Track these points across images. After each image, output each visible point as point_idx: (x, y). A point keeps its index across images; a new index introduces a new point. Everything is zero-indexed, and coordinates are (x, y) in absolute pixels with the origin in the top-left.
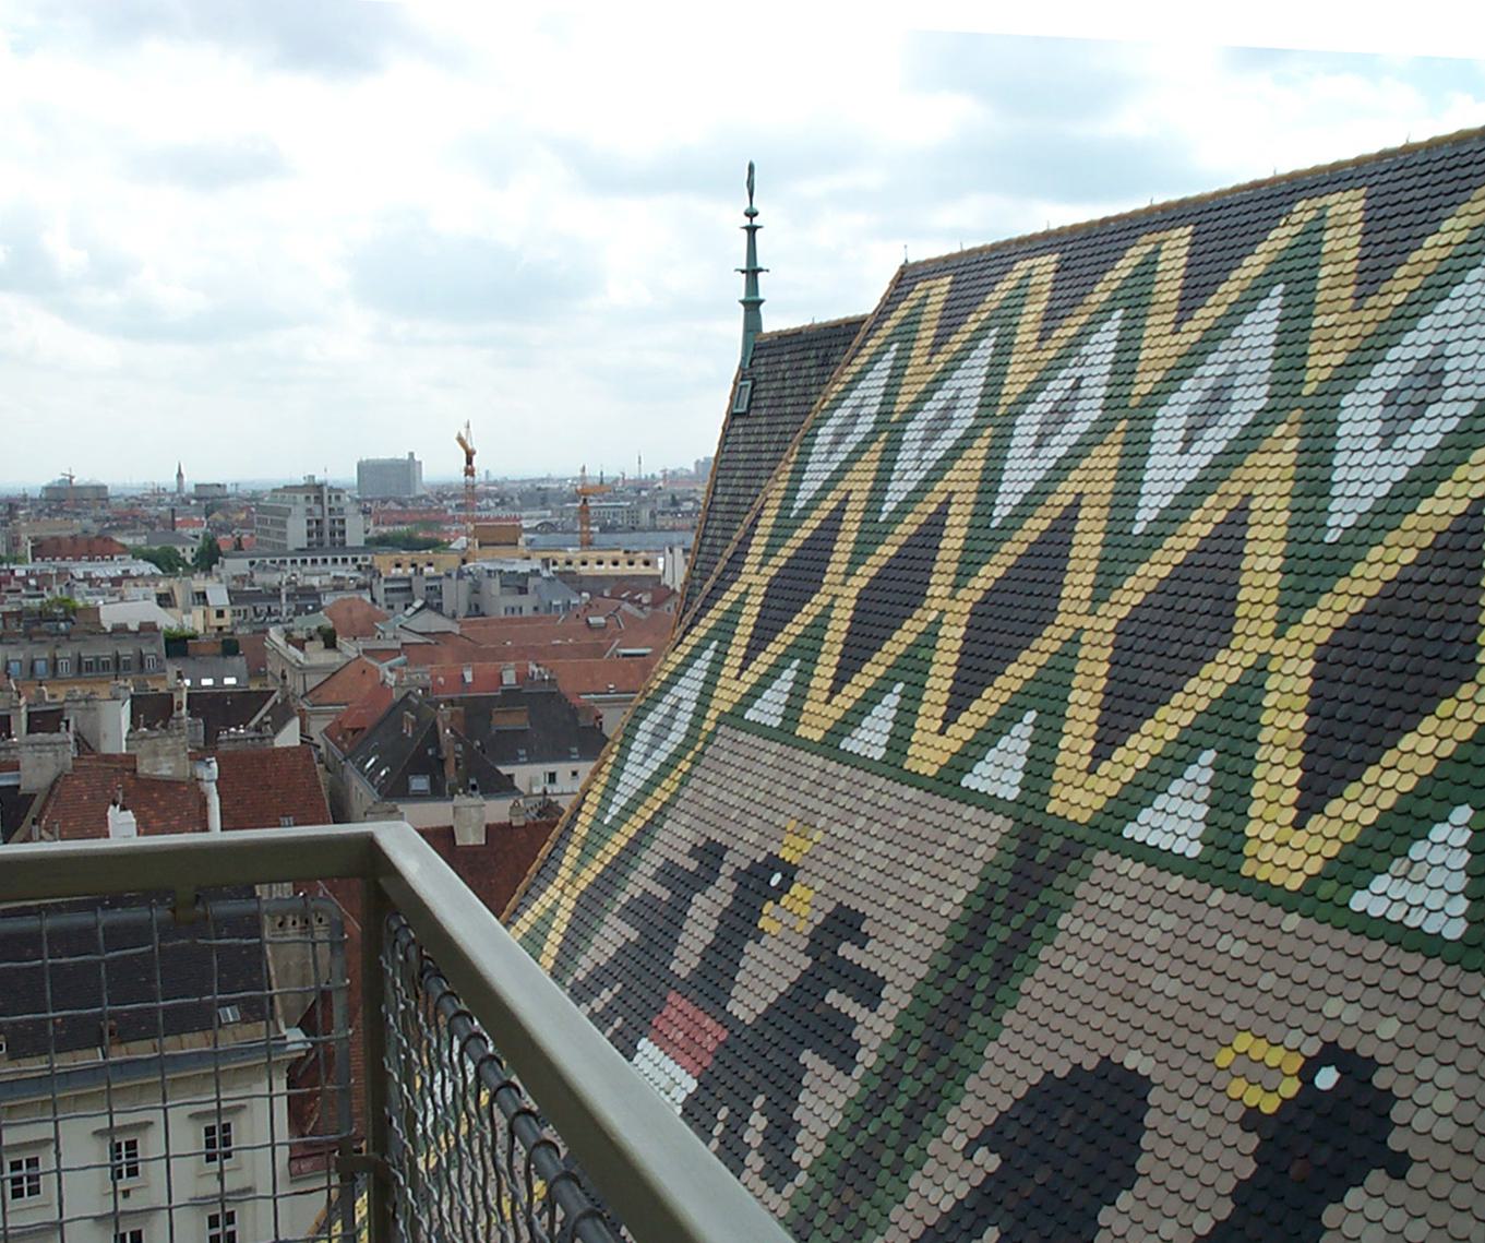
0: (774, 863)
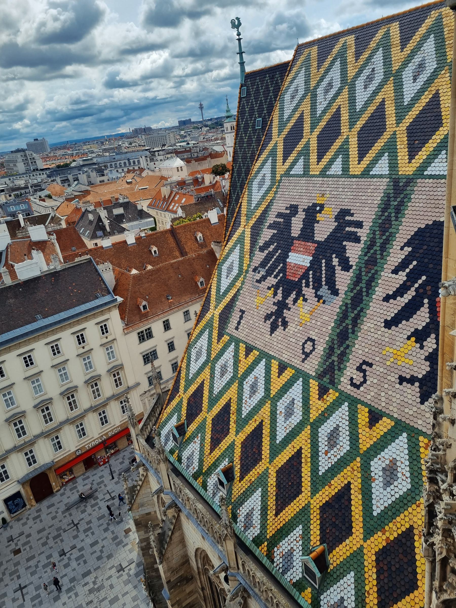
0: (315, 205)
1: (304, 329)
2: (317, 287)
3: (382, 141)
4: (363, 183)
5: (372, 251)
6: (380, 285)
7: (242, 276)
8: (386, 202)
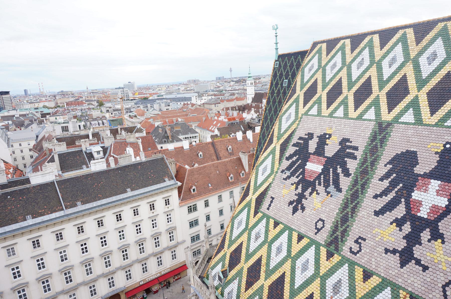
0: (325, 134)
1: (316, 213)
2: (327, 186)
3: (370, 99)
4: (358, 123)
5: (365, 166)
6: (371, 188)
7: (273, 175)
8: (374, 136)
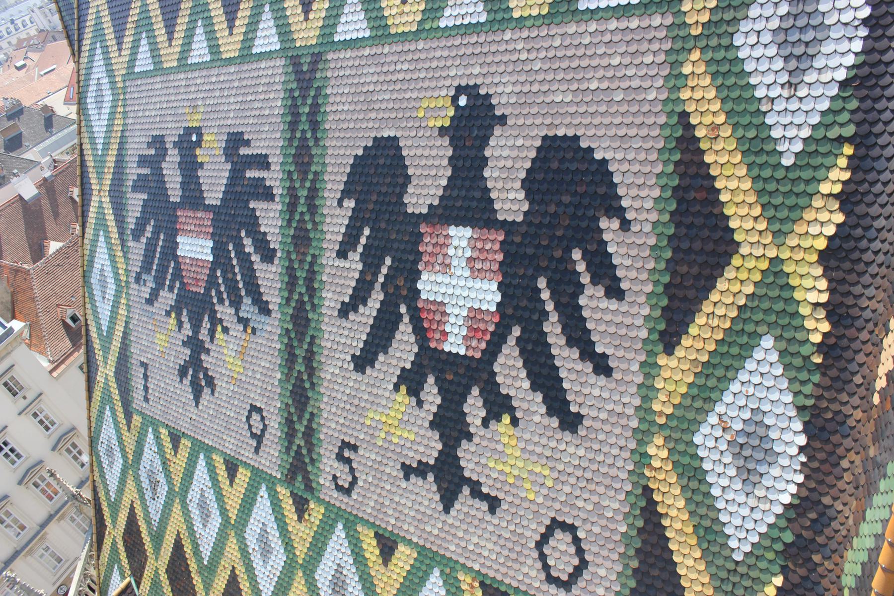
0: (188, 131)
2: (236, 303)
